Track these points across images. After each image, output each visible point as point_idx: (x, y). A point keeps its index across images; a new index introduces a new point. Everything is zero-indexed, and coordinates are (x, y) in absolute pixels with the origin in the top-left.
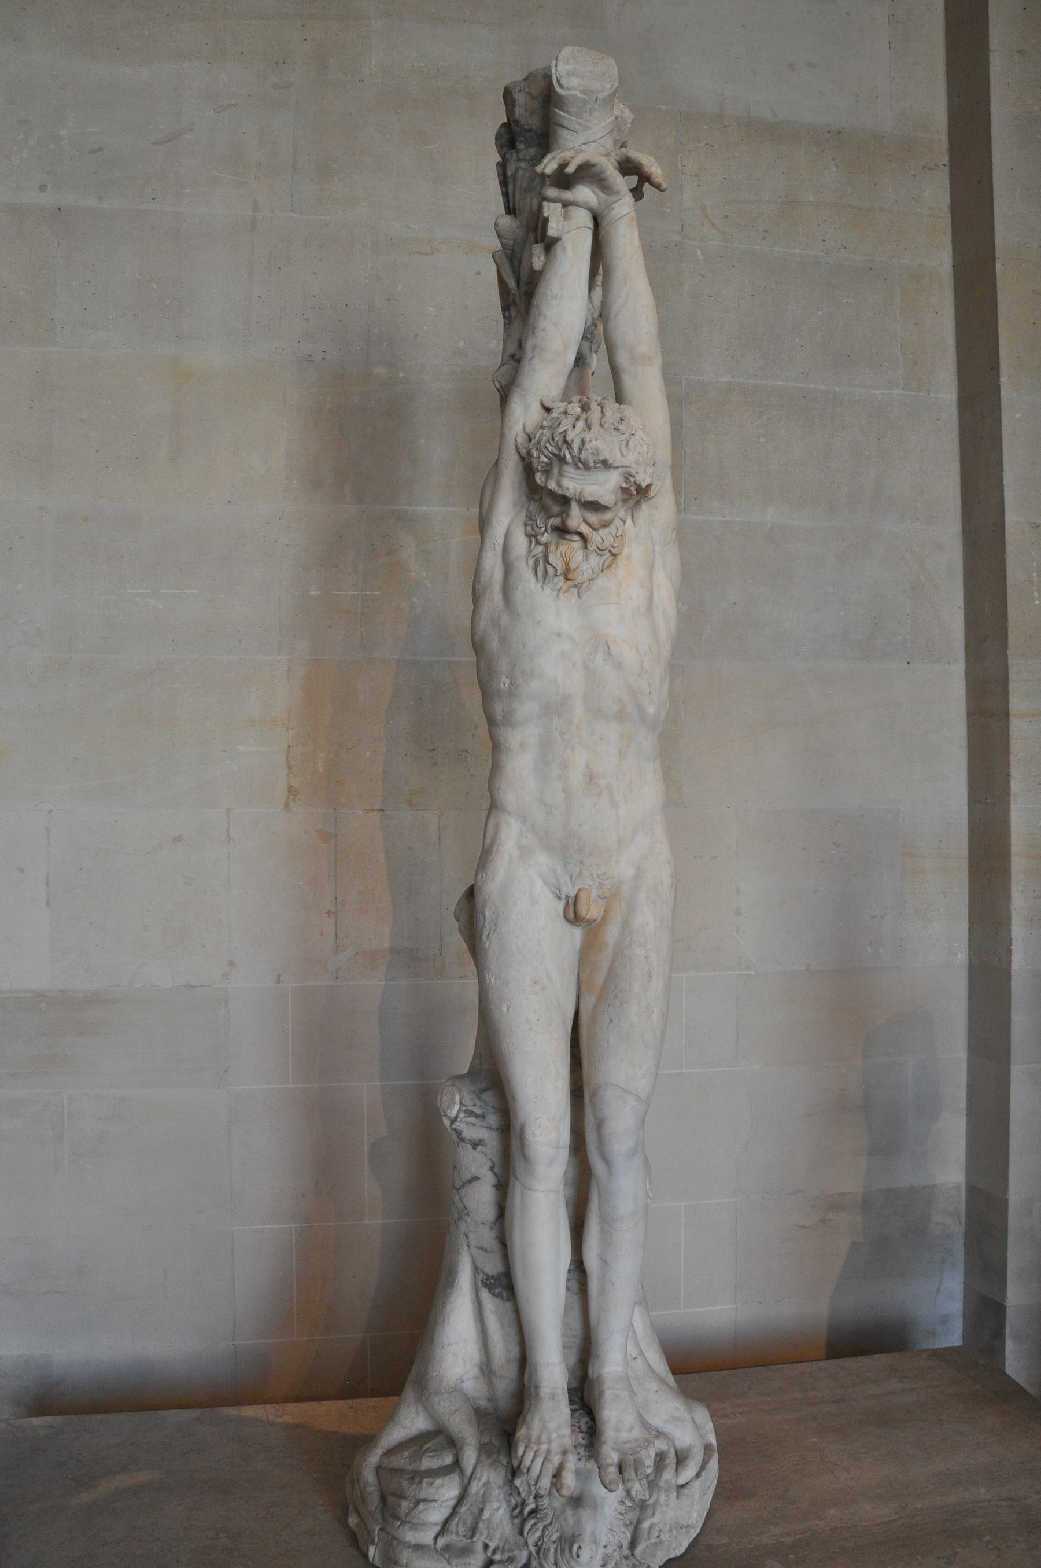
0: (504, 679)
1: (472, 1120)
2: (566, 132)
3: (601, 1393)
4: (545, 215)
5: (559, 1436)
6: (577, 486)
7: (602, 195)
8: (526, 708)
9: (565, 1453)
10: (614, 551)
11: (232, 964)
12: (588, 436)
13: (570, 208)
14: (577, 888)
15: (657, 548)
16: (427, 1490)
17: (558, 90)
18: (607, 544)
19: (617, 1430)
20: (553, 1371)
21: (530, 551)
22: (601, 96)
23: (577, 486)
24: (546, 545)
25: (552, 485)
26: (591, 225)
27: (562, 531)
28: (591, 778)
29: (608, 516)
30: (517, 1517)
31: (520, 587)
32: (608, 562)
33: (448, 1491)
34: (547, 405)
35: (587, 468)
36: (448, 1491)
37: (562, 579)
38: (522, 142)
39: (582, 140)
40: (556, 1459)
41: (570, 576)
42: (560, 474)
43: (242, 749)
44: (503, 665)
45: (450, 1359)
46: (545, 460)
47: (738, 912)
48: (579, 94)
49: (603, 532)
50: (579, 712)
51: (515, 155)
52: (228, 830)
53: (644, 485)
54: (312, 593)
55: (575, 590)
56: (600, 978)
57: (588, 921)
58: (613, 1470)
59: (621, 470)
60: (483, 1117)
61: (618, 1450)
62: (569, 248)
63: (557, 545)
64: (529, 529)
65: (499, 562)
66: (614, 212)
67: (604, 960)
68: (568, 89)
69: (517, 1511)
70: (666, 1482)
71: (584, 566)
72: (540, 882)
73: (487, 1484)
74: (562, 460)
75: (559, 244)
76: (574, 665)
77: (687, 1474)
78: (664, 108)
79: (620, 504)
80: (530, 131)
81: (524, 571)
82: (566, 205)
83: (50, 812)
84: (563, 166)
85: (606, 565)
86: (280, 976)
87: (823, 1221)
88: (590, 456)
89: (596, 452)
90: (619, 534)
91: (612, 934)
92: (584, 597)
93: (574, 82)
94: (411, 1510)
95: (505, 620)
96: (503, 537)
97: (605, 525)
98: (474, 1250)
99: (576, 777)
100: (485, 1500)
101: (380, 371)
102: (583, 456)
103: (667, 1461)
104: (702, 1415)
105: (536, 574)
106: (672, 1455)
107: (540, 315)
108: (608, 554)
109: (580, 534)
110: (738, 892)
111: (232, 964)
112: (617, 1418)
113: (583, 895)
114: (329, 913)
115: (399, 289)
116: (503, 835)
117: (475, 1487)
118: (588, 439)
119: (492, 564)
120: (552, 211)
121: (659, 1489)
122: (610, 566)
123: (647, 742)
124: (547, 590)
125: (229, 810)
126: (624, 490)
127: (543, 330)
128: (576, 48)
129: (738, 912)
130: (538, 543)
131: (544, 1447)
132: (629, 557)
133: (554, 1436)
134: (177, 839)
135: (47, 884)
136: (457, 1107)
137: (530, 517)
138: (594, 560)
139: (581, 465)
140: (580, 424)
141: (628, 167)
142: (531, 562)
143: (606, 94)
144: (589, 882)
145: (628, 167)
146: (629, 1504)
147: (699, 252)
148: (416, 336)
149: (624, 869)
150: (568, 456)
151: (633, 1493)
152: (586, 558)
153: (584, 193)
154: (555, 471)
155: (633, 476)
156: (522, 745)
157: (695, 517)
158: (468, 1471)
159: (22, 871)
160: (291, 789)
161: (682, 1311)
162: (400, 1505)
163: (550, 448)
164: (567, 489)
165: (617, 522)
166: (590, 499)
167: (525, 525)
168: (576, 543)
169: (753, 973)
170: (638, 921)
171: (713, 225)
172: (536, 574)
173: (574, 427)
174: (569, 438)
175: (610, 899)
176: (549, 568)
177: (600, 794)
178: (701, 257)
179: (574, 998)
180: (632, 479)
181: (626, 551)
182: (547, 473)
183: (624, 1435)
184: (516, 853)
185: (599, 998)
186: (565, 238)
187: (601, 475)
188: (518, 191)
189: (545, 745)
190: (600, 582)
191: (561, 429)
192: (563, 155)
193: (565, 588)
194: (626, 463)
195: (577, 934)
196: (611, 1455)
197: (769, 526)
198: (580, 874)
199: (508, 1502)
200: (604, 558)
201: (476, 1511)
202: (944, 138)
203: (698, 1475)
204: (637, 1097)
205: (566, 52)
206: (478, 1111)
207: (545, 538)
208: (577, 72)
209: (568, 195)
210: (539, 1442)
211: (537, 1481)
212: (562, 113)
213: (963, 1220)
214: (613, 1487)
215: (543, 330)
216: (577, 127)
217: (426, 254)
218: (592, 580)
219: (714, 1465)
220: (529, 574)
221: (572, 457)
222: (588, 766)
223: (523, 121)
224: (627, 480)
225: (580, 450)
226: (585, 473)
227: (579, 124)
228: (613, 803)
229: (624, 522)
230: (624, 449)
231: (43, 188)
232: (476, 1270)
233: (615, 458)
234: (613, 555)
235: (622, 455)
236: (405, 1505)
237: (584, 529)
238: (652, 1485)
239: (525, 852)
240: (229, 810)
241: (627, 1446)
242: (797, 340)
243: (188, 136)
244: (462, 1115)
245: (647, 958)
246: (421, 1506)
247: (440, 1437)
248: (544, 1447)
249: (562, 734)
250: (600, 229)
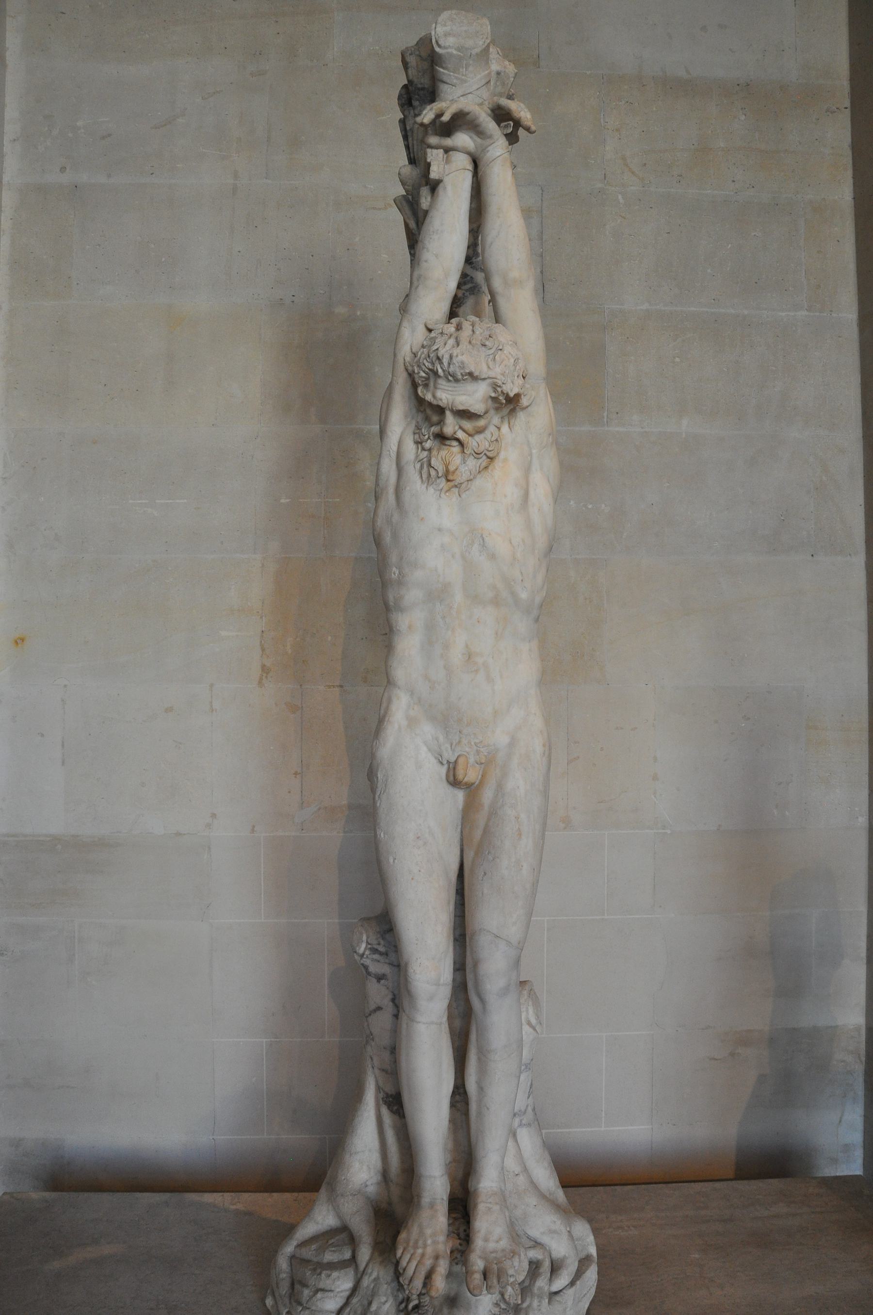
0: (394, 569)
1: (376, 956)
2: (446, 86)
3: (476, 1205)
4: (428, 160)
5: (435, 1242)
6: (448, 396)
7: (479, 140)
8: (412, 595)
9: (437, 1258)
10: (490, 454)
11: (214, 816)
12: (455, 352)
13: (451, 153)
14: (456, 755)
15: (534, 451)
16: (325, 1281)
17: (437, 49)
18: (482, 449)
19: (486, 1240)
20: (436, 1184)
21: (417, 456)
22: (474, 52)
23: (448, 396)
24: (430, 450)
25: (429, 397)
26: (470, 167)
27: (442, 438)
28: (469, 656)
29: (481, 423)
30: (402, 1311)
31: (408, 488)
32: (484, 464)
33: (343, 1283)
34: (430, 327)
35: (457, 380)
36: (343, 1283)
37: (444, 480)
39: (460, 92)
40: (428, 1263)
41: (450, 477)
42: (435, 388)
43: (223, 633)
44: (394, 558)
45: (357, 1165)
46: (424, 375)
47: (655, 778)
48: (455, 52)
49: (478, 438)
50: (459, 597)
51: (412, 112)
52: (211, 702)
53: (512, 395)
54: (283, 501)
55: (456, 490)
56: (478, 834)
57: (466, 784)
58: (477, 1277)
59: (488, 381)
60: (386, 954)
61: (485, 1259)
62: (449, 188)
63: (439, 450)
64: (417, 436)
65: (394, 466)
66: (488, 155)
67: (481, 819)
68: (445, 48)
69: (403, 1305)
70: (540, 1288)
71: (463, 469)
72: (425, 749)
73: (376, 1279)
74: (436, 373)
75: (441, 185)
76: (453, 556)
77: (560, 1283)
78: (588, 73)
79: (492, 412)
80: (423, 89)
81: (412, 473)
82: (447, 150)
83: (65, 686)
84: (439, 115)
85: (482, 467)
86: (254, 827)
87: (732, 1054)
88: (458, 370)
89: (462, 365)
90: (494, 438)
91: (487, 796)
92: (464, 496)
93: (451, 41)
94: (311, 1298)
95: (396, 518)
96: (397, 445)
97: (480, 431)
98: (376, 1071)
99: (456, 655)
100: (374, 1294)
101: (341, 310)
102: (451, 369)
103: (541, 1270)
104: (582, 1229)
105: (421, 477)
106: (547, 1265)
108: (484, 457)
109: (458, 440)
110: (655, 759)
111: (214, 816)
112: (489, 1229)
113: (461, 761)
114: (296, 774)
115: (357, 239)
116: (393, 708)
117: (366, 1282)
118: (455, 354)
119: (388, 467)
120: (435, 157)
121: (532, 1296)
122: (486, 468)
123: (522, 624)
124: (431, 490)
125: (212, 685)
126: (495, 400)
127: (426, 261)
128: (454, 12)
129: (655, 778)
130: (423, 449)
131: (420, 1251)
132: (505, 460)
133: (429, 1242)
134: (169, 710)
135: (63, 746)
136: (364, 946)
137: (418, 427)
138: (472, 463)
139: (450, 378)
140: (451, 342)
141: (501, 115)
142: (418, 466)
143: (478, 50)
144: (467, 749)
145: (501, 115)
146: (503, 1306)
147: (620, 197)
148: (371, 280)
149: (500, 738)
150: (440, 371)
151: (507, 1297)
152: (464, 461)
153: (463, 139)
154: (432, 384)
155: (500, 386)
156: (410, 627)
157: (617, 429)
158: (362, 1267)
159: (42, 735)
160: (264, 669)
161: (603, 1129)
162: (303, 1292)
163: (427, 364)
164: (441, 400)
165: (492, 428)
166: (461, 408)
167: (414, 434)
168: (456, 448)
169: (669, 832)
170: (510, 785)
171: (633, 173)
172: (421, 477)
173: (445, 344)
174: (440, 355)
175: (487, 764)
176: (432, 470)
177: (477, 671)
178: (621, 201)
179: (459, 853)
180: (499, 389)
181: (502, 455)
182: (426, 386)
183: (491, 1245)
184: (404, 723)
185: (477, 853)
186: (447, 180)
187: (470, 387)
189: (430, 627)
190: (478, 482)
191: (435, 347)
192: (440, 106)
193: (446, 488)
194: (491, 374)
195: (460, 795)
196: (478, 1263)
197: (684, 436)
198: (460, 742)
199: (396, 1297)
200: (481, 460)
201: (366, 1303)
202: (846, 84)
203: (572, 1283)
204: (509, 943)
205: (445, 15)
206: (381, 949)
207: (428, 445)
208: (452, 32)
209: (448, 142)
210: (416, 1247)
211: (411, 1281)
212: (442, 70)
213: (864, 1059)
214: (475, 1292)
215: (426, 261)
216: (455, 81)
217: (380, 209)
218: (471, 480)
219: (592, 1275)
220: (416, 477)
221: (444, 371)
222: (467, 646)
224: (495, 391)
225: (449, 364)
226: (455, 385)
227: (456, 78)
228: (489, 679)
229: (499, 428)
230: (491, 364)
231: (63, 169)
232: (378, 1089)
233: (481, 369)
234: (488, 457)
235: (489, 367)
236: (306, 1292)
237: (460, 435)
238: (525, 1290)
239: (412, 722)
240: (212, 685)
241: (494, 1255)
242: (709, 271)
243: (180, 120)
244: (367, 952)
245: (517, 818)
246: (319, 1295)
247: (343, 1234)
248: (420, 1251)
249: (444, 618)
250: (480, 168)
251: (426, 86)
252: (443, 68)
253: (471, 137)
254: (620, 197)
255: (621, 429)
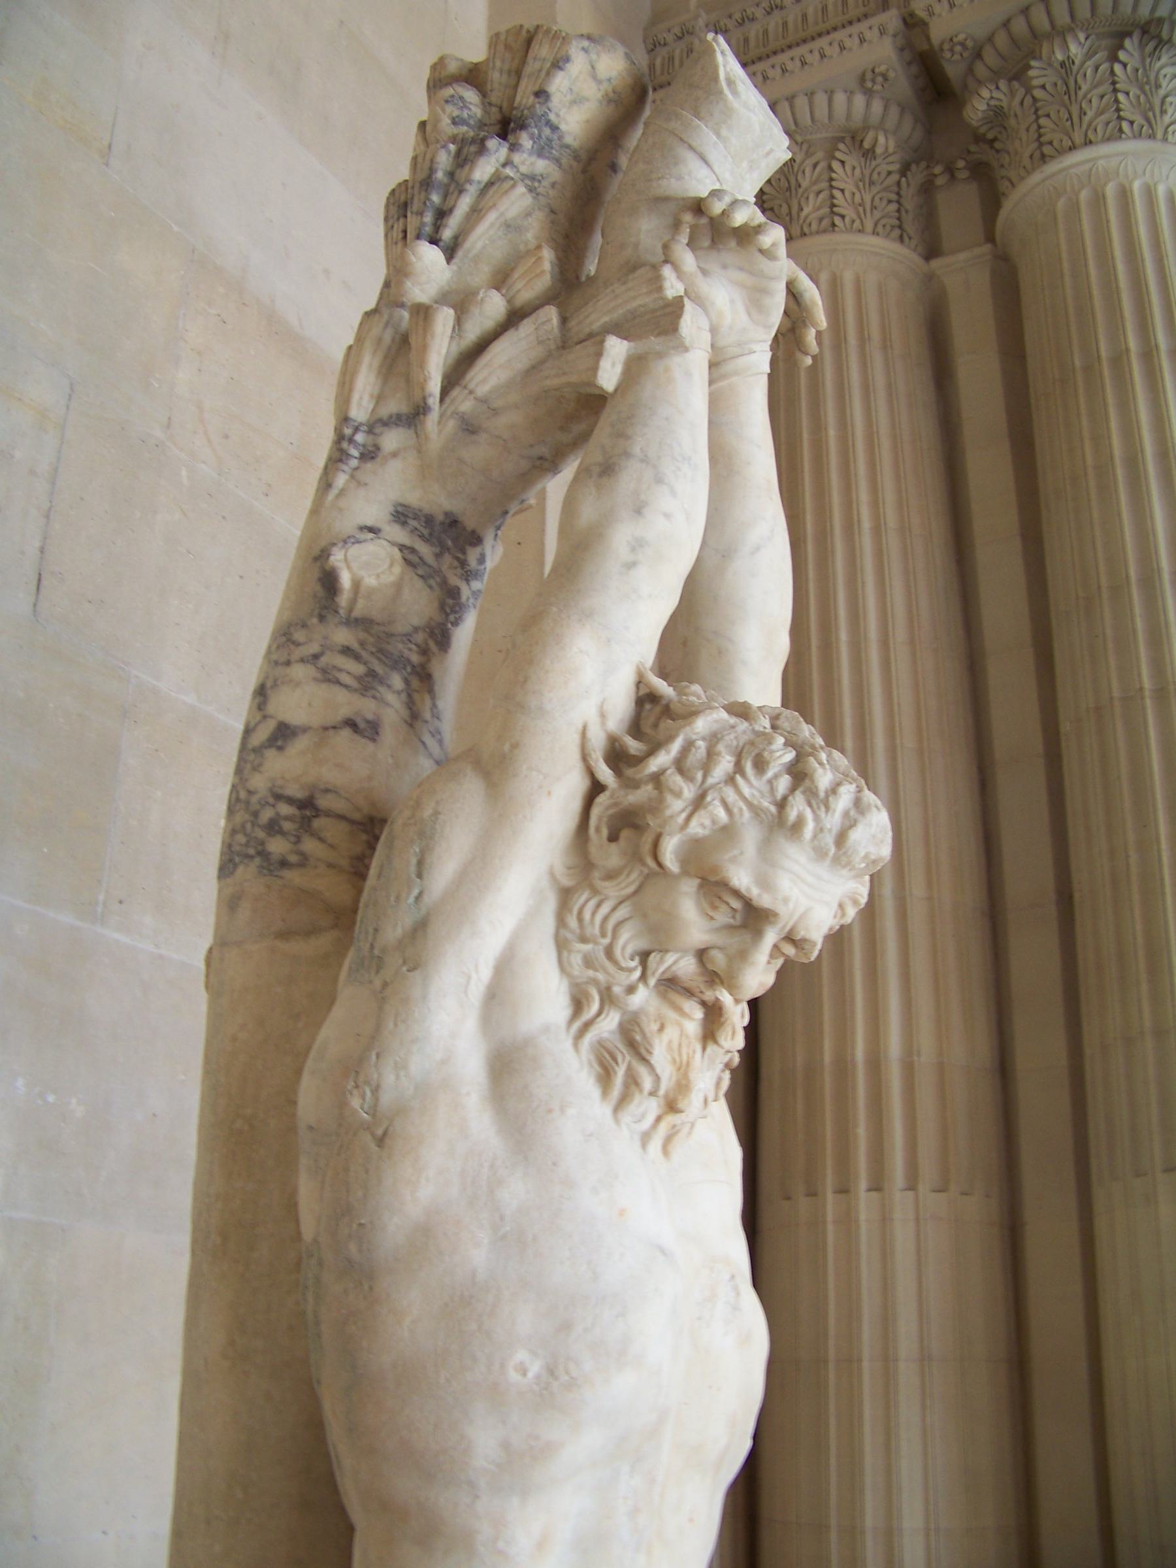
0: (521, 1355)
7: (744, 317)
31: (571, 1111)
38: (532, 137)
46: (722, 814)
65: (471, 1024)
80: (555, 128)
95: (516, 1191)
107: (659, 480)
127: (667, 516)
147: (184, 473)
157: (116, 935)
163: (746, 791)
164: (786, 900)
171: (209, 441)
188: (492, 217)
220: (584, 1080)
221: (819, 830)
223: (556, 101)
251: (563, 127)
252: (718, 135)
253: (732, 302)
254: (184, 473)
255: (123, 938)
